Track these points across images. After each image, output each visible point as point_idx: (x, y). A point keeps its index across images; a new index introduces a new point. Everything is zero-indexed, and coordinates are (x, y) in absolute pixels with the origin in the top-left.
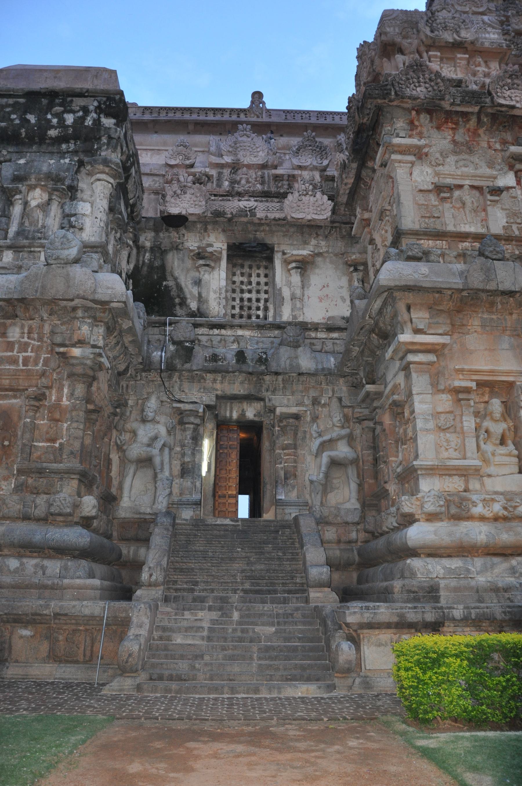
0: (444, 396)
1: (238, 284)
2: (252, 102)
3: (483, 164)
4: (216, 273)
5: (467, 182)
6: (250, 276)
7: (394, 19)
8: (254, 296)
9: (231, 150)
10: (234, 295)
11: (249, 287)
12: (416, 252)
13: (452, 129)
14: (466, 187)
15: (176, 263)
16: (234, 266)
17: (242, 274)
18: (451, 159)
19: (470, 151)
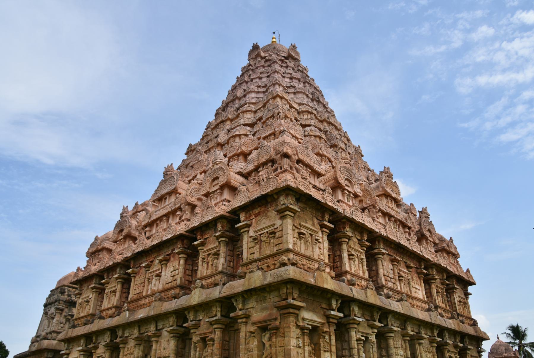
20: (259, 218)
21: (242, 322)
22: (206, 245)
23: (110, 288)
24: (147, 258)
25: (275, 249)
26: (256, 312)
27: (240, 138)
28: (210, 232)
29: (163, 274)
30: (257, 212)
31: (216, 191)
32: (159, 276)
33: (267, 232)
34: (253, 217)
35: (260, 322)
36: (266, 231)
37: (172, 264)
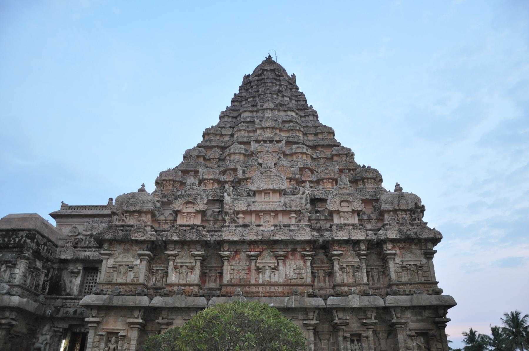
0: (97, 337)
1: (89, 280)
2: (109, 203)
3: (131, 257)
4: (78, 278)
5: (124, 264)
6: (94, 276)
7: (118, 201)
8: (93, 285)
9: (90, 229)
10: (87, 285)
11: (92, 281)
12: (98, 291)
13: (124, 244)
14: (124, 266)
15: (65, 275)
16: (89, 273)
17: (91, 276)
18: (122, 255)
19: (128, 252)
20: (403, 251)
21: (401, 327)
22: (342, 257)
23: (182, 263)
24: (250, 247)
25: (423, 279)
26: (412, 321)
27: (307, 157)
28: (348, 247)
29: (281, 268)
30: (401, 246)
31: (347, 212)
32: (276, 269)
33: (413, 265)
34: (398, 249)
35: (420, 330)
36: (412, 263)
37: (293, 262)
